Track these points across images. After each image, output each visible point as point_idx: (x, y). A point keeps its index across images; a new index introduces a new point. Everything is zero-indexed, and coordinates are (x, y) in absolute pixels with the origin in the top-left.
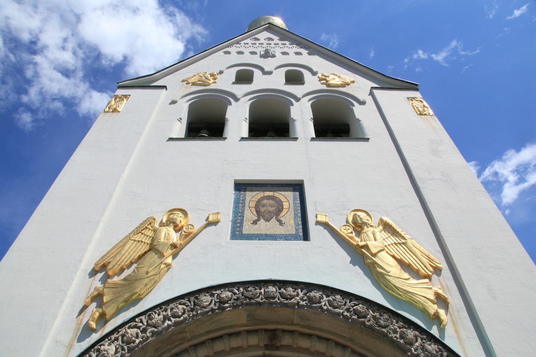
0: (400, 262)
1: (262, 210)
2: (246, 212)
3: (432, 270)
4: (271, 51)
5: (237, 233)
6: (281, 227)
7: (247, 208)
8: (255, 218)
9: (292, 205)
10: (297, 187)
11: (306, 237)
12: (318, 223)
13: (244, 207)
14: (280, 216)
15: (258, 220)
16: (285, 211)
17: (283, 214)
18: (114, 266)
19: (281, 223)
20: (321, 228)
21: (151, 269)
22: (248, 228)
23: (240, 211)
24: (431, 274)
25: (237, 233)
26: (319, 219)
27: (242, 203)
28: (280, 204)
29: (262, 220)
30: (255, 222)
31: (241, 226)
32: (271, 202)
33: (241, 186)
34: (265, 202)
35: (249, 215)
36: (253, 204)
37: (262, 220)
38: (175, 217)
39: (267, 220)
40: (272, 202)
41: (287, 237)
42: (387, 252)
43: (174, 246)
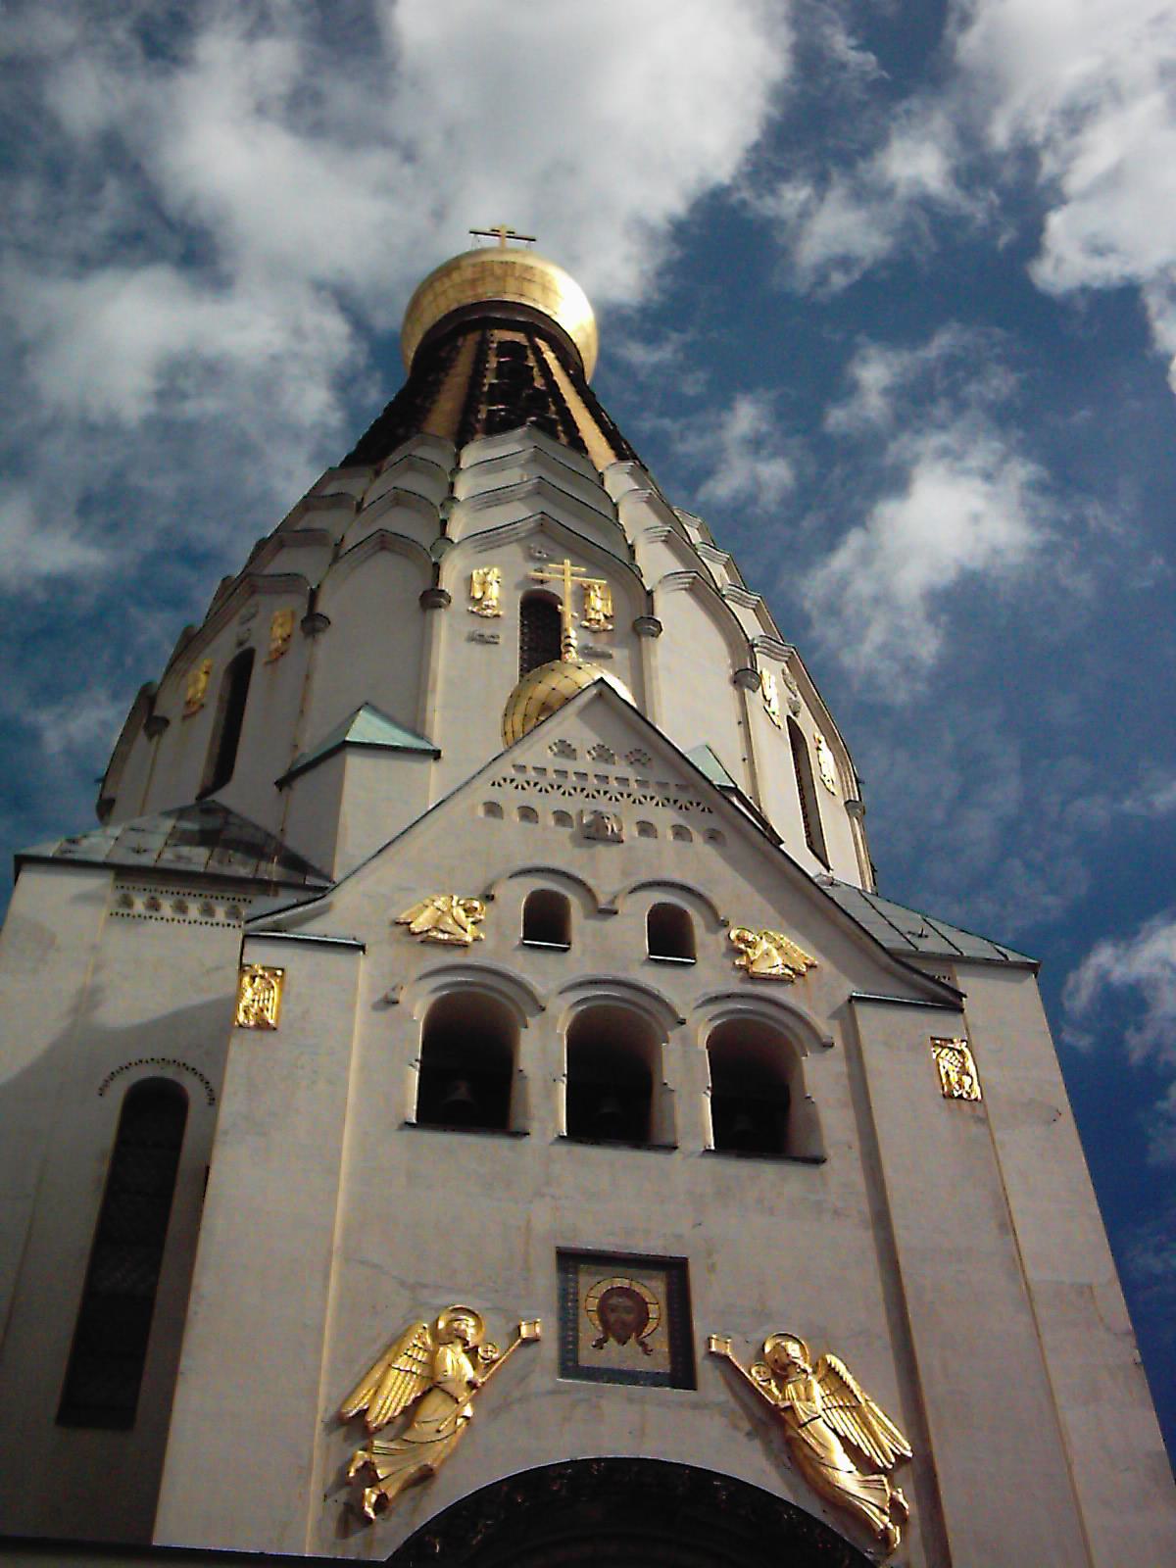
0: (844, 1441)
1: (612, 1318)
2: (581, 1320)
3: (893, 1460)
4: (612, 825)
5: (570, 1366)
6: (646, 1357)
10: (675, 1270)
14: (644, 1334)
16: (652, 1324)
17: (647, 1330)
18: (377, 1417)
19: (647, 1351)
21: (442, 1427)
22: (587, 1356)
23: (571, 1317)
24: (890, 1467)
26: (713, 1349)
27: (571, 1301)
28: (642, 1307)
29: (612, 1341)
30: (600, 1344)
32: (628, 1303)
33: (570, 1260)
34: (614, 1301)
35: (590, 1328)
36: (593, 1304)
37: (612, 1341)
38: (463, 1327)
39: (622, 1341)
40: (631, 1307)
41: (655, 1380)
42: (824, 1421)
43: (472, 1385)
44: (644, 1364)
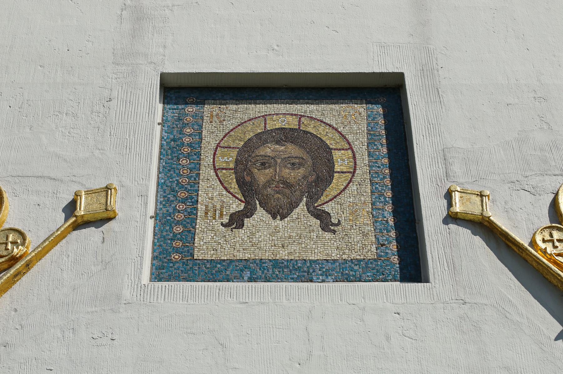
1: (261, 176)
2: (203, 185)
5: (176, 260)
6: (328, 235)
7: (206, 172)
8: (236, 206)
9: (363, 159)
11: (412, 266)
12: (452, 218)
13: (198, 167)
14: (323, 198)
15: (248, 212)
16: (338, 182)
17: (331, 191)
19: (326, 222)
20: (463, 234)
23: (184, 181)
25: (176, 260)
27: (188, 156)
29: (260, 214)
30: (236, 221)
31: (190, 233)
32: (292, 150)
34: (269, 150)
36: (228, 159)
37: (260, 214)
39: (279, 213)
41: (348, 271)
44: (324, 247)
